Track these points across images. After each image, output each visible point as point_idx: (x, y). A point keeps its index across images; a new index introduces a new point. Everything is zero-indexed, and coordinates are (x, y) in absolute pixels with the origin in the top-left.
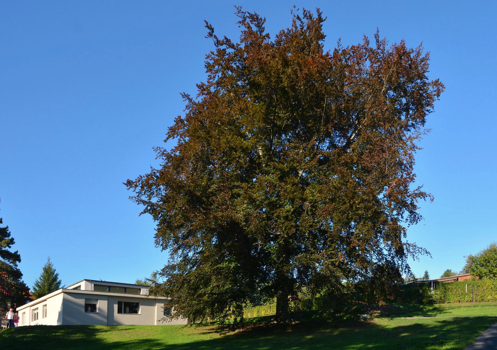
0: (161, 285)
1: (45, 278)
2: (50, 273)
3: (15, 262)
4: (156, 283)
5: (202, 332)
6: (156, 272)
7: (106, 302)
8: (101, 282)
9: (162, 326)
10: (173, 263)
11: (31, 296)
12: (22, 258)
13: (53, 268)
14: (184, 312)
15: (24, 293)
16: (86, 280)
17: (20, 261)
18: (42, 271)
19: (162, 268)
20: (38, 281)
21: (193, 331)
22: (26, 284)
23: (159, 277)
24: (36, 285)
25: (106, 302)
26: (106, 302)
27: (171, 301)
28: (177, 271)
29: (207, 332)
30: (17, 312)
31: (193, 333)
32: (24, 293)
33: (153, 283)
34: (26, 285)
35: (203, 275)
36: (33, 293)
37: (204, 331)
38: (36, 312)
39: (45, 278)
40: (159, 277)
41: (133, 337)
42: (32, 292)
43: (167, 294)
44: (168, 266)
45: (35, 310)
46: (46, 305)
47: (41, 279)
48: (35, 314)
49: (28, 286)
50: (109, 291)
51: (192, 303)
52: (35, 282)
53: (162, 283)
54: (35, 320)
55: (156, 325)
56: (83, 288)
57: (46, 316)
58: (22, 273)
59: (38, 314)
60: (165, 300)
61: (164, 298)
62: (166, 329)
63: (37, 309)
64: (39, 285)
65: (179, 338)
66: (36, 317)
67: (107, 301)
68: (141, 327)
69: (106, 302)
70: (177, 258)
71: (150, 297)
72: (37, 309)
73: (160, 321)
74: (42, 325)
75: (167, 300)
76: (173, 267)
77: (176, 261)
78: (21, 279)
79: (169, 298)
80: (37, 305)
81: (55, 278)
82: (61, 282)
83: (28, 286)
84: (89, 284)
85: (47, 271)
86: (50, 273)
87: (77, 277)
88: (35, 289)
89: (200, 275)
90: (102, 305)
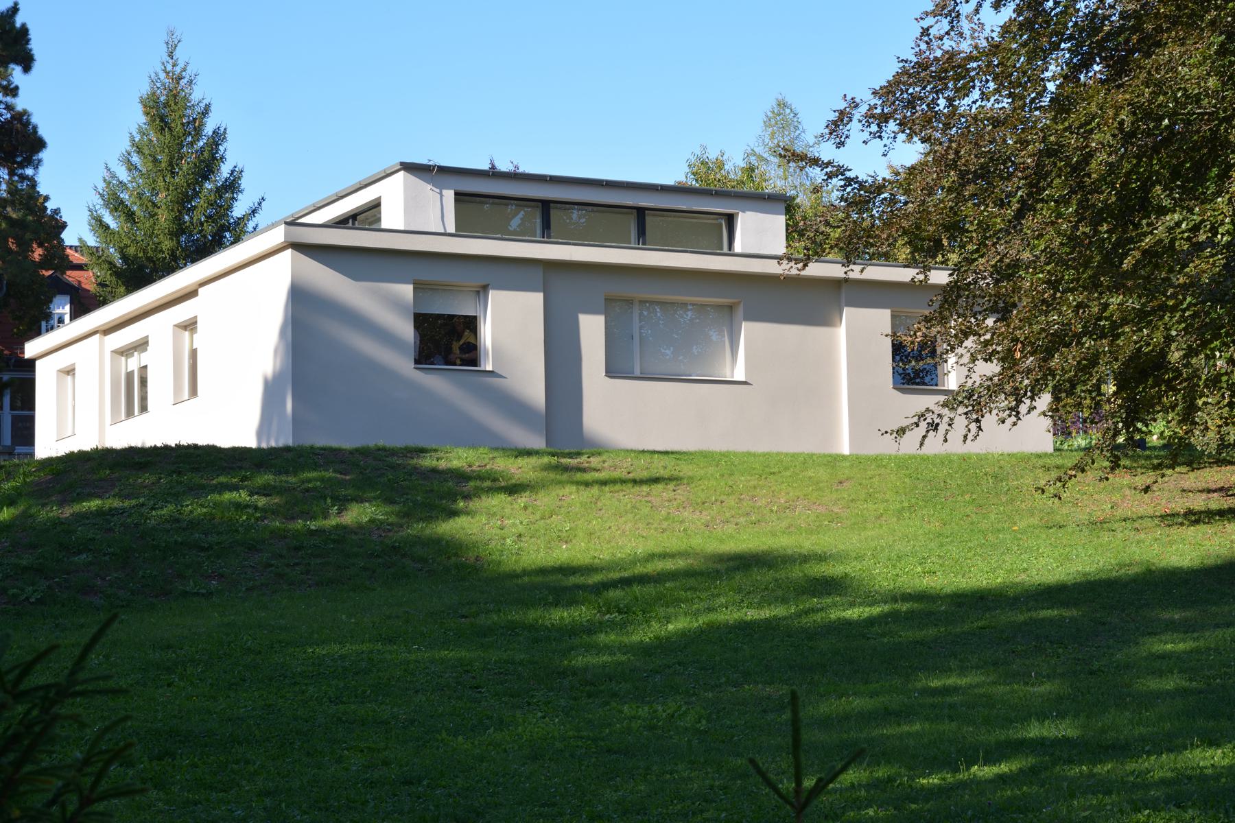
0: (879, 189)
1: (155, 161)
2: (178, 129)
3: (6, 67)
4: (849, 181)
5: (1179, 505)
6: (842, 105)
7: (535, 300)
8: (493, 174)
9: (902, 463)
10: (948, 44)
11: (80, 267)
12: (36, 45)
13: (195, 97)
14: (1041, 364)
15: (38, 253)
16: (409, 167)
17: (27, 62)
18: (137, 118)
19: (880, 81)
20: (114, 176)
21: (1116, 497)
22: (47, 198)
23: (866, 135)
24: (107, 205)
25: (537, 299)
26: (537, 299)
27: (950, 295)
28: (976, 94)
29: (1214, 506)
30: (31, 363)
31: (1119, 513)
32: (38, 253)
33: (830, 176)
34: (50, 206)
35: (1173, 116)
36: (93, 252)
37: (1198, 503)
38: (133, 364)
39: (155, 161)
40: (866, 135)
41: (730, 528)
42: (82, 247)
43: (925, 250)
44: (923, 66)
45: (126, 352)
46: (190, 326)
47: (131, 167)
48: (130, 376)
49: (57, 211)
50: (547, 232)
51: (1105, 306)
52: (101, 186)
53: (884, 174)
54: (130, 413)
55: (846, 450)
56: (392, 217)
57: (194, 392)
58: (42, 132)
59: (144, 382)
60: (911, 285)
61: (905, 275)
62: (930, 485)
63: (142, 345)
64: (122, 202)
65: (1032, 543)
66: (134, 395)
67: (539, 297)
68: (771, 468)
69: (535, 300)
70: (977, 11)
71: (816, 269)
72: (142, 345)
73: (902, 431)
74: (196, 447)
75: (924, 286)
76: (948, 72)
77: (967, 33)
78: (36, 168)
79: (940, 277)
80: (149, 322)
81: (209, 162)
82: (244, 183)
83: (57, 211)
84: (426, 189)
85: (162, 119)
86: (178, 129)
87: (323, 149)
88: (99, 225)
89: (1148, 115)
90: (509, 327)
